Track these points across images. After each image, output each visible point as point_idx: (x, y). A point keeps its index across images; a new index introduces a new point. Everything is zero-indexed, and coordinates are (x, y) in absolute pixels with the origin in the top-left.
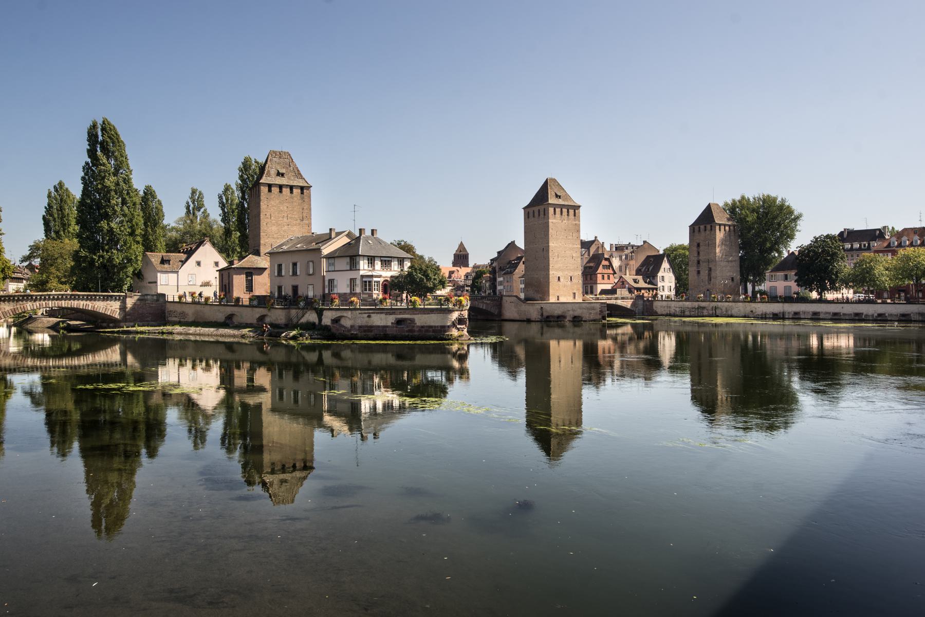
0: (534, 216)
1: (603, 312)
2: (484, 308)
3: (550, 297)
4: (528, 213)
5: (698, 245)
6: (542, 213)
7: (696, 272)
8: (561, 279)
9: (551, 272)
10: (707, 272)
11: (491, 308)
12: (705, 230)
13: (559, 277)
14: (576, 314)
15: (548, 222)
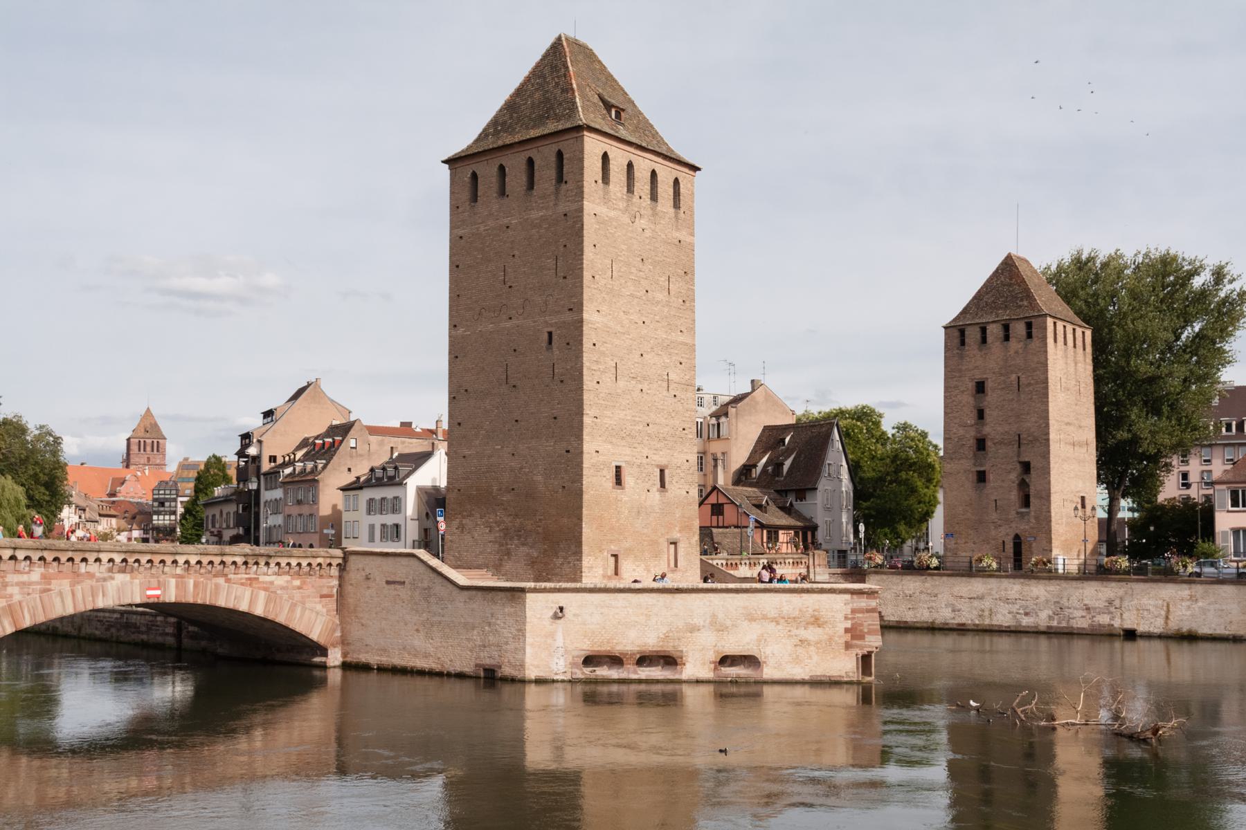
0: (502, 192)
1: (862, 637)
2: (259, 611)
3: (586, 561)
4: (474, 176)
5: (980, 387)
6: (545, 174)
7: (973, 477)
8: (628, 479)
9: (589, 446)
10: (1014, 476)
11: (293, 606)
12: (1007, 338)
13: (618, 468)
14: (733, 647)
15: (581, 210)
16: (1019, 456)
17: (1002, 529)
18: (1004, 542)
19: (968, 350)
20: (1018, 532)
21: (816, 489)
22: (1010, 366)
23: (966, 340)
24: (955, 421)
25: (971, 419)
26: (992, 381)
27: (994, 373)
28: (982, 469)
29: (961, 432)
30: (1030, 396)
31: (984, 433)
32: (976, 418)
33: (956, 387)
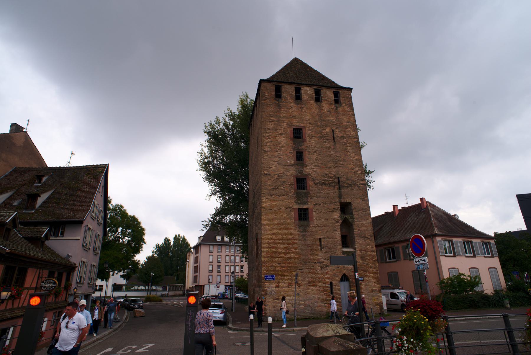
5: (298, 133)
7: (294, 214)
16: (340, 196)
17: (329, 269)
18: (331, 283)
19: (285, 102)
20: (344, 272)
21: (81, 222)
22: (325, 121)
23: (283, 95)
24: (274, 159)
25: (291, 159)
26: (310, 130)
27: (310, 124)
28: (305, 207)
29: (281, 169)
30: (344, 147)
31: (304, 173)
32: (295, 159)
33: (274, 129)
